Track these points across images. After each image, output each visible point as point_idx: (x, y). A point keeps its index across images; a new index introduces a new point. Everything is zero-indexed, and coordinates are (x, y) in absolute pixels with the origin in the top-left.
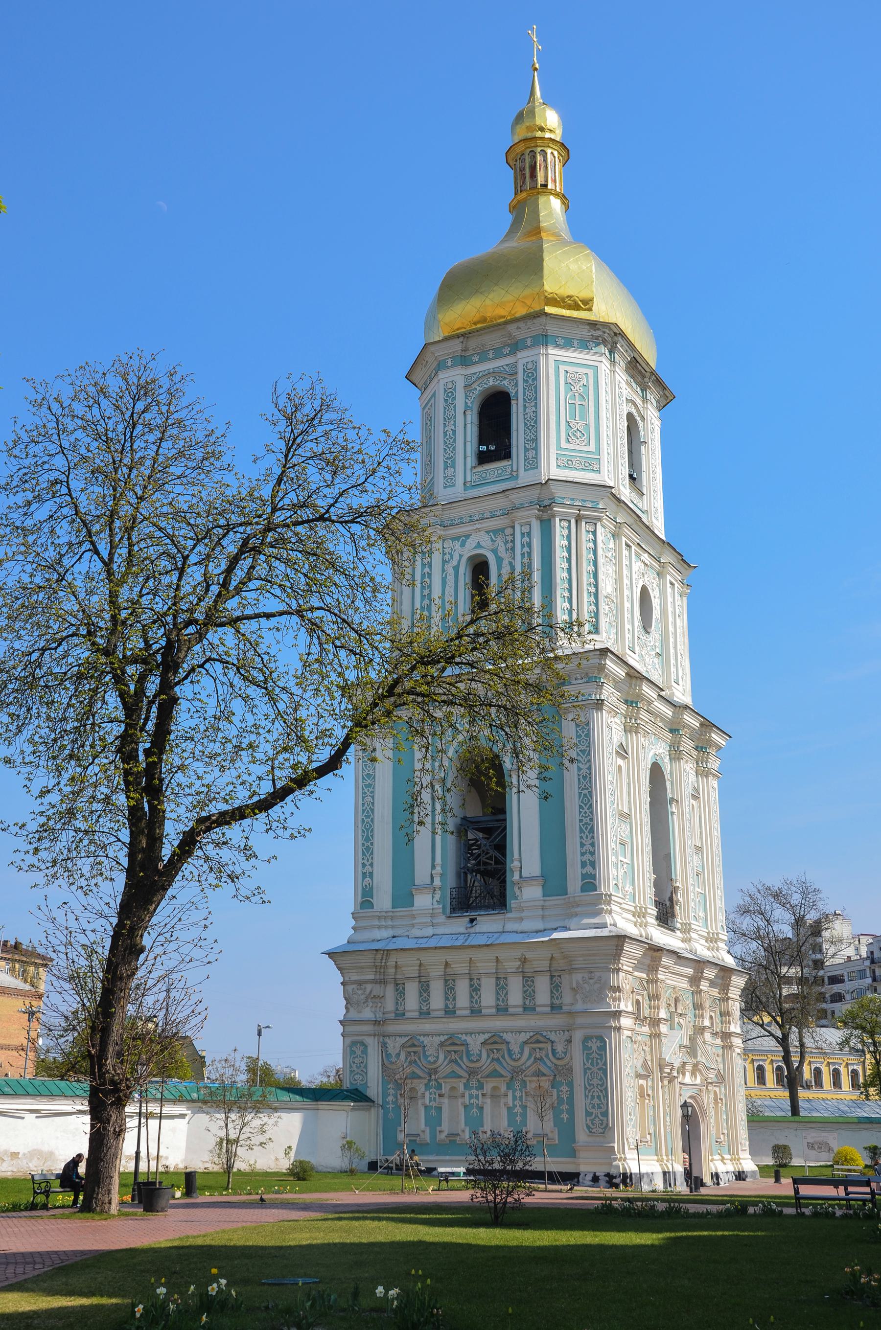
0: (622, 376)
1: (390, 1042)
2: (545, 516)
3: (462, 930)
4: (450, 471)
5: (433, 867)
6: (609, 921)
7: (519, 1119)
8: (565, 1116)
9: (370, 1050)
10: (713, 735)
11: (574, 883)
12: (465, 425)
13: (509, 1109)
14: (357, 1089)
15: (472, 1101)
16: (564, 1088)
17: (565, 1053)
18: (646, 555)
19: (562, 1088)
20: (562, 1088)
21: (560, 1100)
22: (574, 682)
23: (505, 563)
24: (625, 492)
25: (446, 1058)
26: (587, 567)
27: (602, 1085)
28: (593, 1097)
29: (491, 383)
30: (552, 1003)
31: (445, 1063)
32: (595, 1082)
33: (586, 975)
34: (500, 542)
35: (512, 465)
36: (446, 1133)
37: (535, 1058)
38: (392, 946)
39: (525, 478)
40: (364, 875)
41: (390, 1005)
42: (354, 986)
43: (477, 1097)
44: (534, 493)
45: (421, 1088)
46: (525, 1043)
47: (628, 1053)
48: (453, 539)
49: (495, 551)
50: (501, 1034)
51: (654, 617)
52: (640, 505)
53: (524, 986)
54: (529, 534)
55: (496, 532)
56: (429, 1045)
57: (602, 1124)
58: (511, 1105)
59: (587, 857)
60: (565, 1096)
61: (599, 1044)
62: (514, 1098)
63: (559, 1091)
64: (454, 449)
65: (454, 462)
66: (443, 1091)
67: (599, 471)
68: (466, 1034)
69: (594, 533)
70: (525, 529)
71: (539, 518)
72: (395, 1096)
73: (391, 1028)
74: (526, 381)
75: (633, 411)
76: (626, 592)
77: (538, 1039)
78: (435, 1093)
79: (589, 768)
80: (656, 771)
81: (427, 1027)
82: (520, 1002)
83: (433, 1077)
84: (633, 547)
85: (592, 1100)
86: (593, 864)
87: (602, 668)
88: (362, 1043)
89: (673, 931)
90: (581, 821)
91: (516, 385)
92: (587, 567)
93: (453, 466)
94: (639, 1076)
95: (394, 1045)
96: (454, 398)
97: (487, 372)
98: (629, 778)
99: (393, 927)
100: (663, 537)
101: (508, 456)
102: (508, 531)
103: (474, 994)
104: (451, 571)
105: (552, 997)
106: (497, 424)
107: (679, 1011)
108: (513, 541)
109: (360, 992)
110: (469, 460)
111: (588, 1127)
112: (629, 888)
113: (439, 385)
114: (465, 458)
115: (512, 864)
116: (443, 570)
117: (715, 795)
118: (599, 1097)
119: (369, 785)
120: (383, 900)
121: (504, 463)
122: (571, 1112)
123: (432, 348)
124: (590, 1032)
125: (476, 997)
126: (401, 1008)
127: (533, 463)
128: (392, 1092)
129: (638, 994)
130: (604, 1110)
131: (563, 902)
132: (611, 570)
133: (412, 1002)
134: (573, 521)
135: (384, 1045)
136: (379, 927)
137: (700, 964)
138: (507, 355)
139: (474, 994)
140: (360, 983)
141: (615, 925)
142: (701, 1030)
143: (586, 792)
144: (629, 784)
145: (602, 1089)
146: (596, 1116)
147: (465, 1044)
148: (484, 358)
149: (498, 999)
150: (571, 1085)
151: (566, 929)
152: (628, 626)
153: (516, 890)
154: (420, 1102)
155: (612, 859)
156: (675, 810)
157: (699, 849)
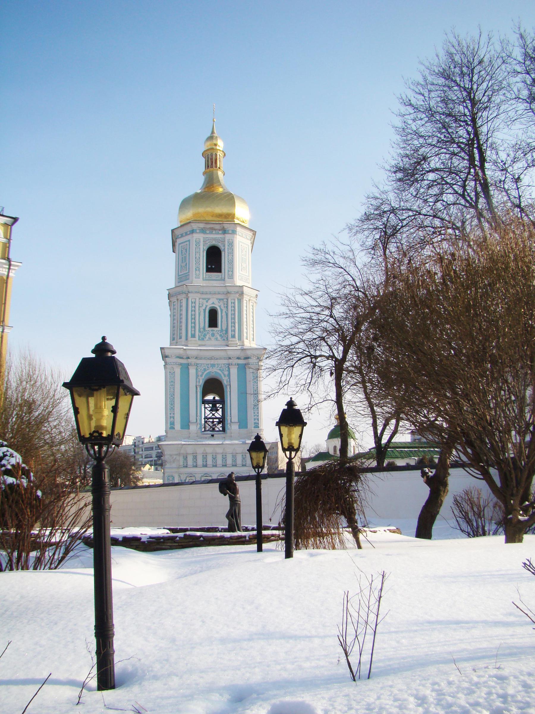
5: (197, 416)
29: (214, 243)
34: (221, 303)
35: (222, 275)
48: (203, 299)
49: (220, 306)
55: (220, 300)
59: (256, 417)
79: (257, 388)
86: (258, 420)
91: (224, 246)
93: (199, 270)
97: (214, 238)
101: (220, 271)
108: (227, 304)
127: (231, 277)
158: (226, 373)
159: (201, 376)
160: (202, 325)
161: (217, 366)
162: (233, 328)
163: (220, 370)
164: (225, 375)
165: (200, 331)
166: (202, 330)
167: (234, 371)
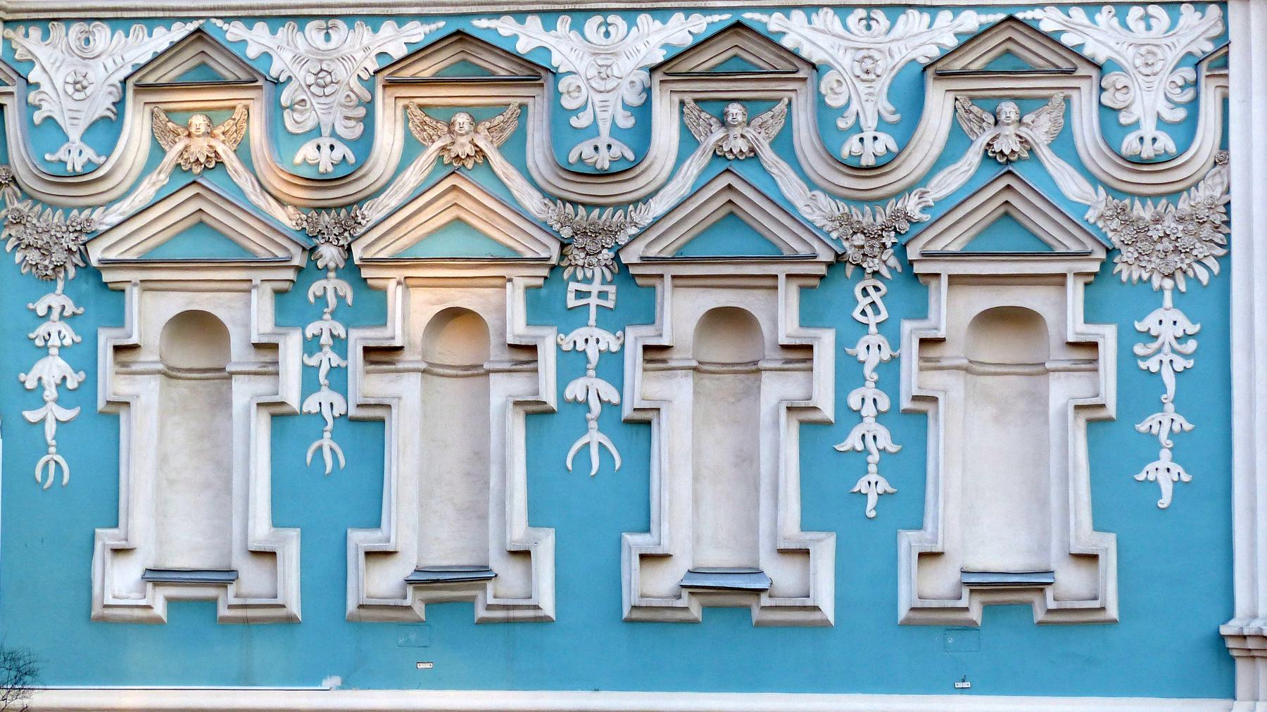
7: (872, 485)
15: (575, 390)
16: (1168, 322)
17: (1187, 129)
19: (1148, 323)
20: (1148, 323)
21: (1139, 387)
31: (412, 177)
37: (990, 156)
43: (612, 365)
46: (937, 69)
50: (774, 23)
56: (303, 75)
58: (828, 412)
60: (1166, 366)
62: (849, 373)
63: (1129, 336)
66: (394, 333)
78: (340, 345)
128: (60, 333)
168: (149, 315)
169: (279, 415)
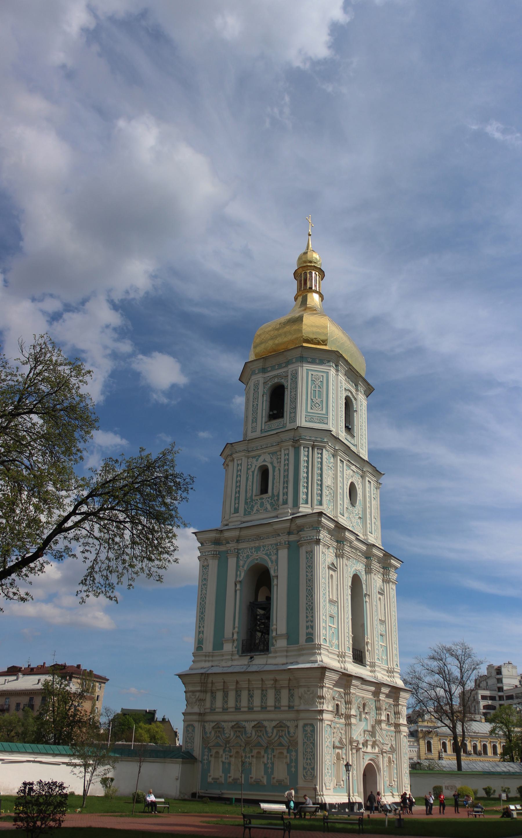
0: (342, 377)
1: (207, 725)
2: (297, 445)
3: (246, 663)
4: (254, 424)
5: (234, 628)
6: (319, 658)
7: (270, 770)
8: (293, 769)
9: (196, 729)
10: (392, 561)
11: (302, 639)
12: (263, 401)
13: (265, 765)
14: (188, 752)
16: (294, 753)
17: (294, 733)
18: (354, 467)
21: (291, 760)
22: (306, 530)
23: (277, 469)
24: (343, 435)
25: (234, 734)
26: (317, 471)
27: (312, 752)
28: (307, 759)
29: (276, 381)
30: (289, 705)
32: (309, 750)
33: (306, 689)
36: (232, 778)
38: (210, 671)
39: (289, 426)
40: (199, 632)
41: (208, 705)
42: (191, 694)
44: (291, 434)
45: (221, 752)
46: (274, 727)
47: (329, 734)
48: (253, 458)
49: (272, 463)
51: (358, 498)
52: (353, 442)
53: (275, 695)
54: (288, 454)
55: (273, 453)
57: (311, 775)
59: (309, 623)
60: (293, 758)
61: (311, 728)
63: (290, 755)
64: (257, 413)
65: (256, 420)
67: (327, 424)
68: (245, 721)
69: (322, 454)
70: (286, 452)
71: (293, 446)
72: (208, 756)
73: (208, 718)
74: (292, 379)
75: (350, 395)
76: (339, 484)
77: (281, 726)
79: (312, 575)
80: (356, 580)
81: (226, 717)
82: (273, 704)
83: (227, 745)
84: (345, 462)
85: (307, 760)
87: (320, 522)
88: (192, 725)
89: (365, 666)
90: (307, 604)
91: (287, 382)
92: (317, 471)
94: (334, 747)
95: (209, 727)
96: (258, 389)
98: (337, 582)
99: (212, 661)
100: (366, 458)
102: (278, 453)
103: (250, 699)
104: (251, 473)
105: (289, 701)
106: (278, 401)
107: (366, 711)
109: (193, 697)
110: (264, 419)
111: (304, 776)
112: (335, 641)
113: (251, 384)
114: (262, 418)
115: (273, 627)
116: (247, 473)
117: (393, 593)
118: (310, 759)
119: (204, 584)
120: (208, 647)
121: (280, 420)
122: (296, 767)
123: (249, 365)
124: (306, 722)
125: (251, 701)
126: (214, 706)
127: (293, 419)
129: (338, 701)
130: (312, 766)
131: (296, 648)
132: (331, 473)
133: (219, 703)
134: (310, 449)
135: (204, 728)
136: (205, 661)
137: (379, 685)
138: (284, 367)
139: (250, 699)
140: (193, 692)
141: (322, 661)
142: (379, 722)
143: (310, 588)
144: (337, 585)
145: (312, 754)
146: (309, 770)
147: (244, 728)
148: (273, 368)
149: (262, 702)
150: (296, 751)
151: (297, 663)
152: (339, 502)
153: (274, 641)
154: (220, 759)
155: (322, 624)
156: (367, 600)
157: (383, 622)
158: (274, 558)
159: (243, 566)
160: (249, 495)
161: (262, 549)
162: (285, 490)
163: (265, 554)
164: (272, 562)
165: (246, 503)
166: (249, 500)
167: (283, 554)
168: (214, 751)
169: (223, 762)
